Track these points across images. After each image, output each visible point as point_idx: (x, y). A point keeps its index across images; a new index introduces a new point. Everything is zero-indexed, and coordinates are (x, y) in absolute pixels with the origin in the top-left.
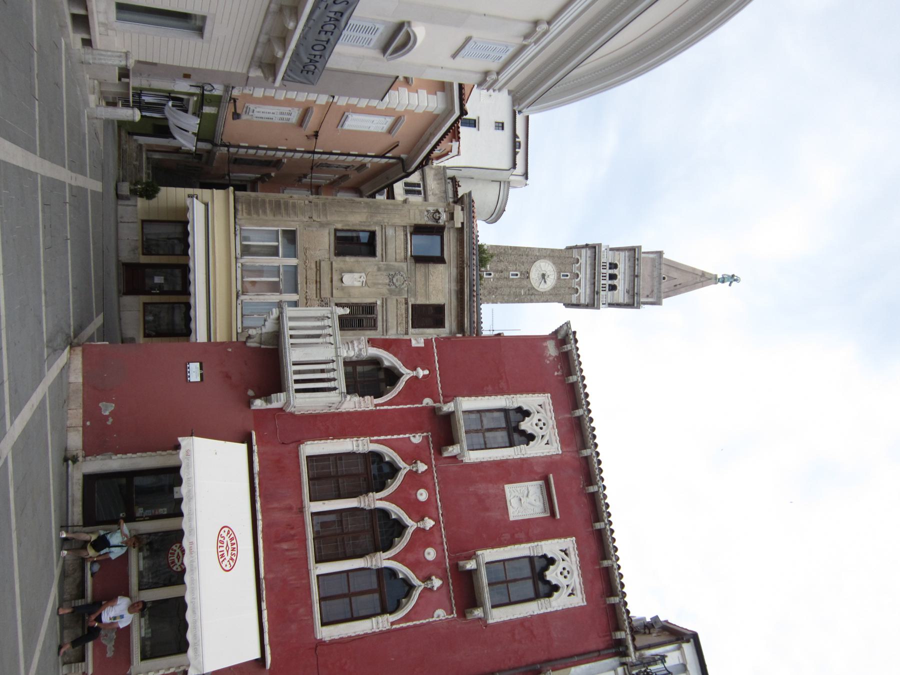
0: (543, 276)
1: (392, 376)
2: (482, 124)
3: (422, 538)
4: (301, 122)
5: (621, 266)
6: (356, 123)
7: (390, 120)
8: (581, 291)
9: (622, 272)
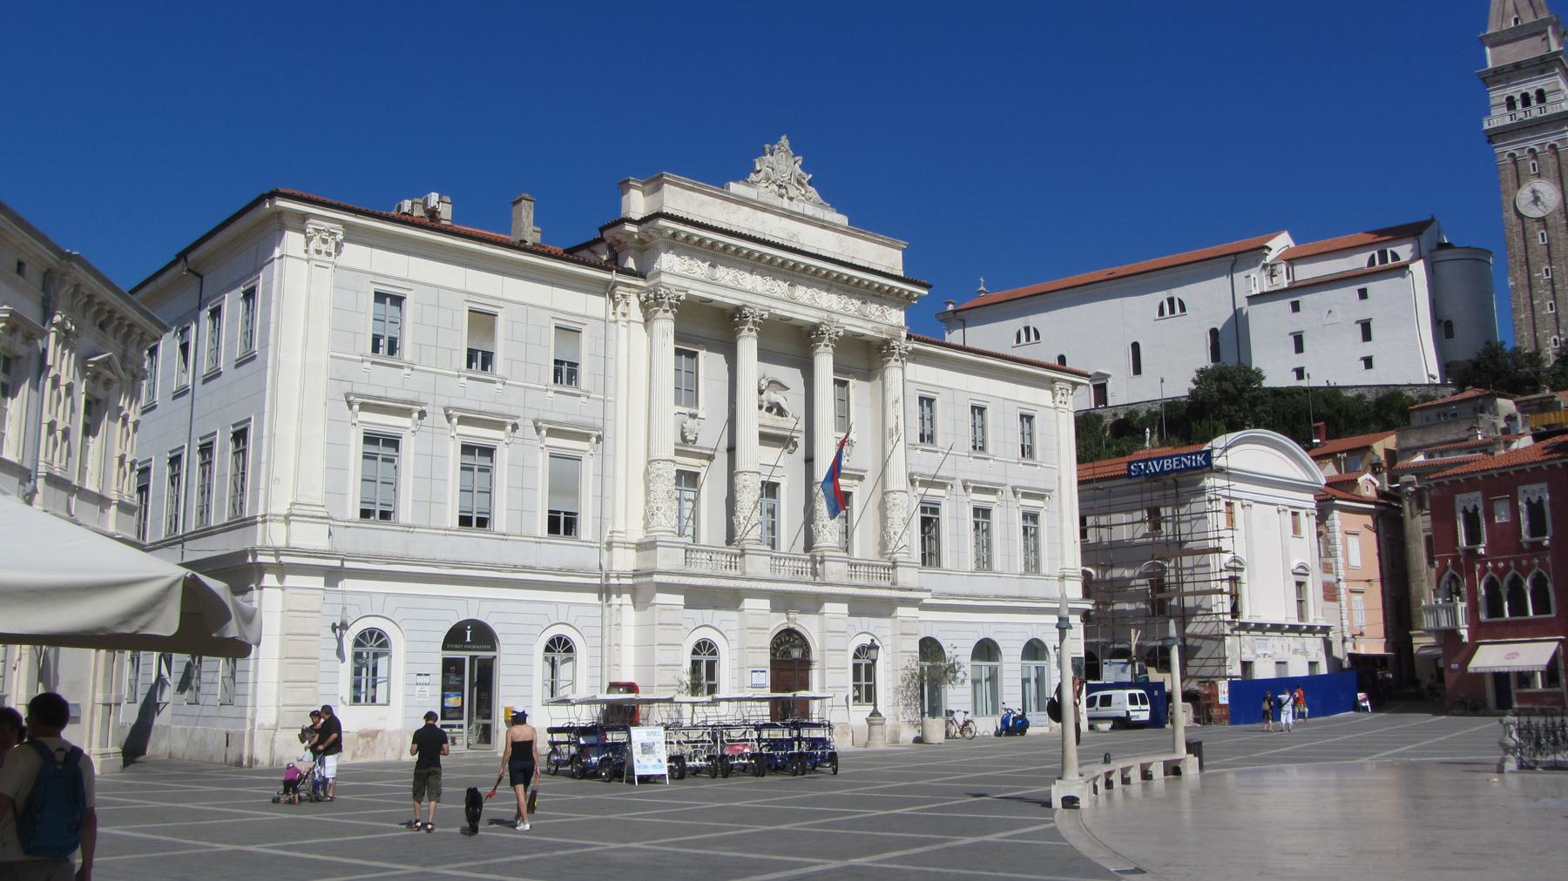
1: (1453, 577)
3: (1518, 566)
5: (1509, 91)
6: (1355, 560)
7: (1350, 538)
8: (1551, 140)
9: (1515, 91)
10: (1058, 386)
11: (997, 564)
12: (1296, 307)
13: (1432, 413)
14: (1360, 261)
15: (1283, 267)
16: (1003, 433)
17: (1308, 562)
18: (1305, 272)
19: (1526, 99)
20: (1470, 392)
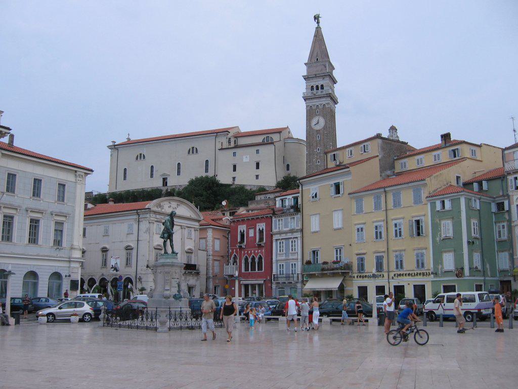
0: (318, 123)
2: (257, 160)
3: (254, 252)
4: (218, 260)
5: (312, 84)
6: (217, 248)
8: (324, 103)
9: (314, 83)
10: (78, 173)
11: (40, 241)
12: (234, 154)
13: (262, 197)
14: (259, 139)
15: (233, 140)
16: (49, 192)
17: (193, 248)
18: (242, 141)
19: (317, 87)
20: (278, 189)
